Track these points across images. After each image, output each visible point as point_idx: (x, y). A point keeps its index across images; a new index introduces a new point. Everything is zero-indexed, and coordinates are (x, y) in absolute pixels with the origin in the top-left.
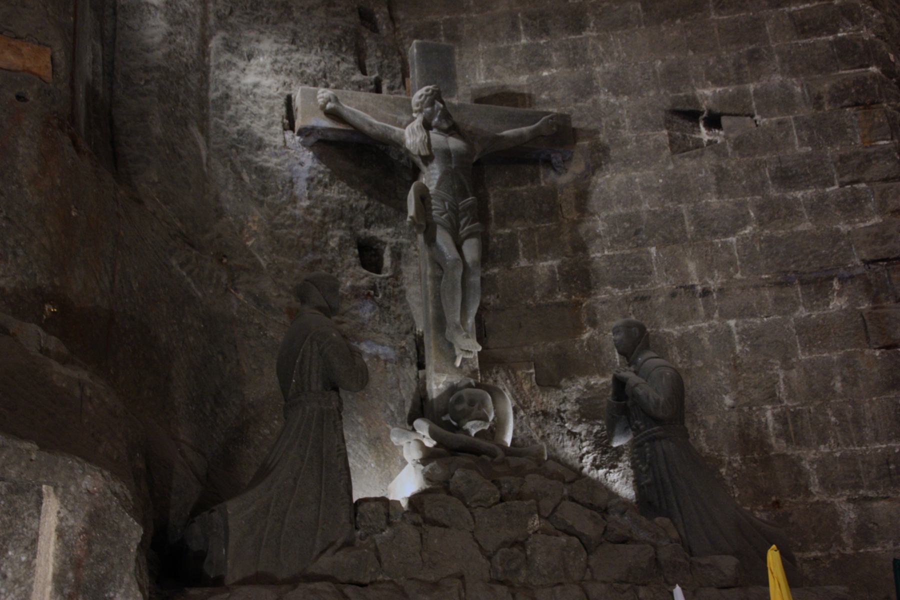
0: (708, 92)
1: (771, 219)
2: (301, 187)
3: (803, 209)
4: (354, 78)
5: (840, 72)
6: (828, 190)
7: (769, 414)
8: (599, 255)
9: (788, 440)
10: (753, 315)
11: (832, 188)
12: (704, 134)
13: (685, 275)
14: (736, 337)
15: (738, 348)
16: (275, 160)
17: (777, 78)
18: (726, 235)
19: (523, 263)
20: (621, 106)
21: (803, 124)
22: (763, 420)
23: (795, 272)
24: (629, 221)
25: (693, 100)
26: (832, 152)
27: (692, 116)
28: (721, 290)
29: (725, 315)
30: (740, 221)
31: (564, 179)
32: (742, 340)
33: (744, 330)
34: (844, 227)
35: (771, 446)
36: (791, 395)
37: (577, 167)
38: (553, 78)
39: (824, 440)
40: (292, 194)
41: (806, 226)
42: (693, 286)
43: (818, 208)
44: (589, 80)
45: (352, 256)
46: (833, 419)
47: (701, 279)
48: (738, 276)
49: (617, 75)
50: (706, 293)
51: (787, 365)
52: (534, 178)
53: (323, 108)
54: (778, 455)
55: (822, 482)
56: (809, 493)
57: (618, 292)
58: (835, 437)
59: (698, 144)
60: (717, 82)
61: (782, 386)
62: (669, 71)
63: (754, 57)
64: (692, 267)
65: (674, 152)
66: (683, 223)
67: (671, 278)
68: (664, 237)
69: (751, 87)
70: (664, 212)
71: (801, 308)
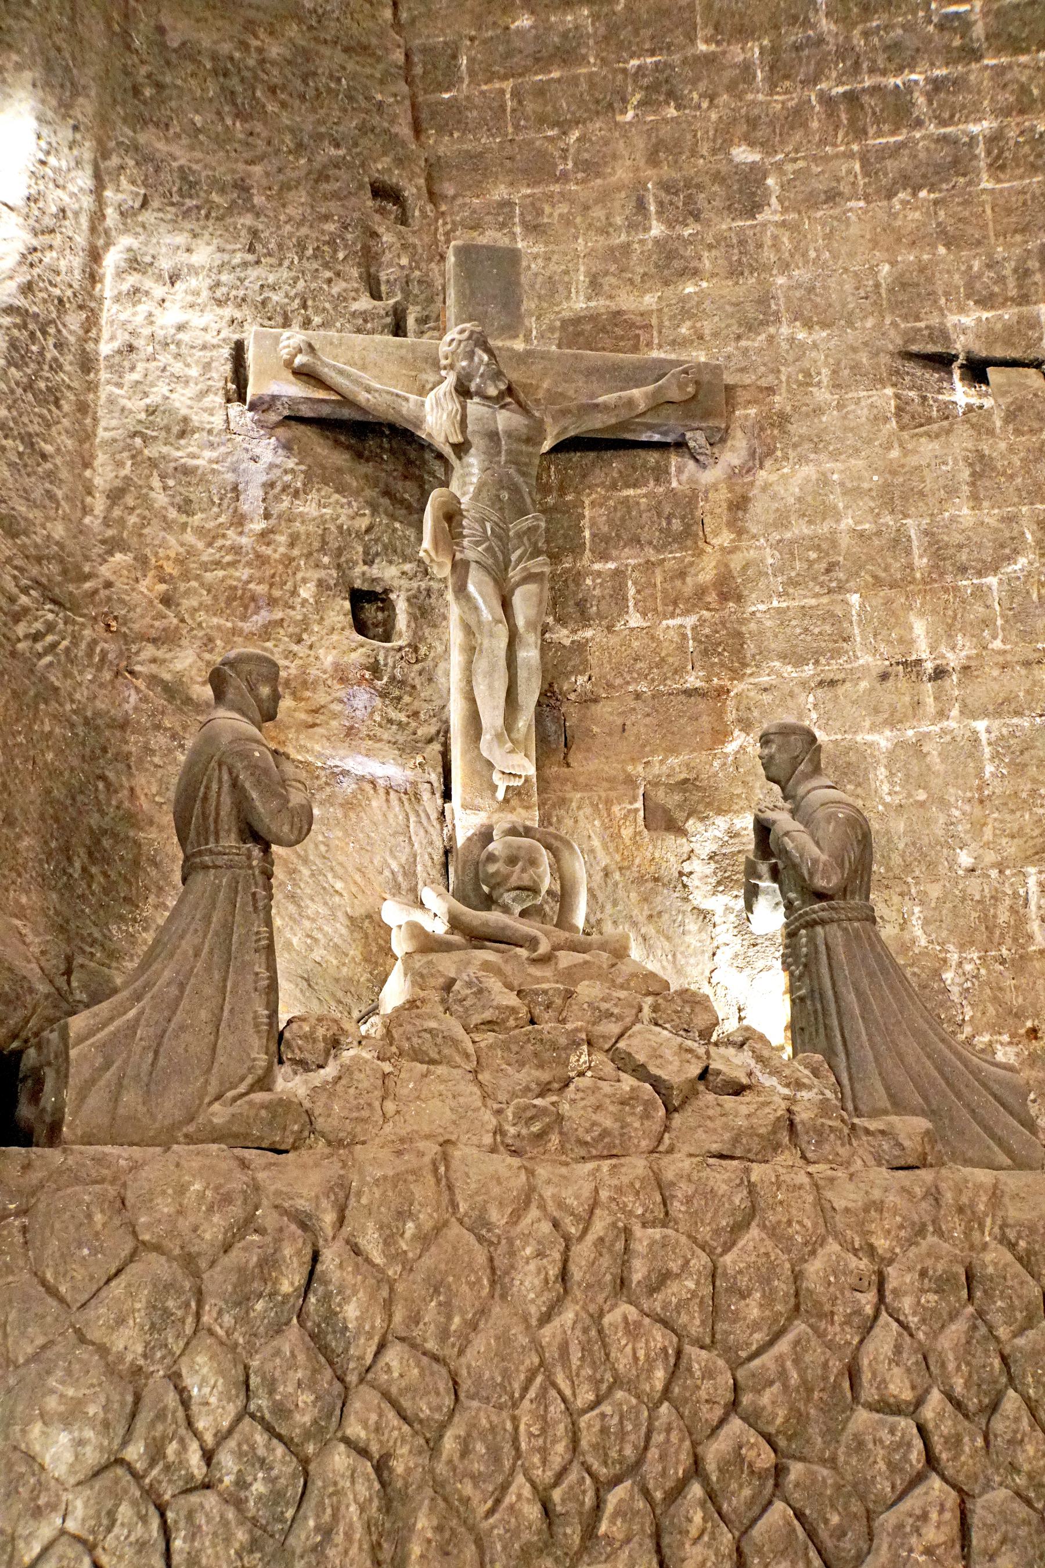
2: (252, 501)
4: (355, 306)
8: (762, 607)
13: (908, 642)
16: (208, 454)
19: (635, 620)
20: (815, 345)
24: (818, 548)
25: (943, 335)
27: (942, 362)
31: (709, 476)
37: (734, 454)
38: (702, 295)
40: (235, 511)
42: (919, 662)
44: (764, 300)
47: (933, 649)
49: (811, 290)
50: (940, 673)
52: (660, 474)
53: (289, 364)
59: (947, 412)
62: (902, 283)
64: (919, 628)
66: (908, 552)
67: (883, 648)
68: (875, 577)
70: (879, 533)
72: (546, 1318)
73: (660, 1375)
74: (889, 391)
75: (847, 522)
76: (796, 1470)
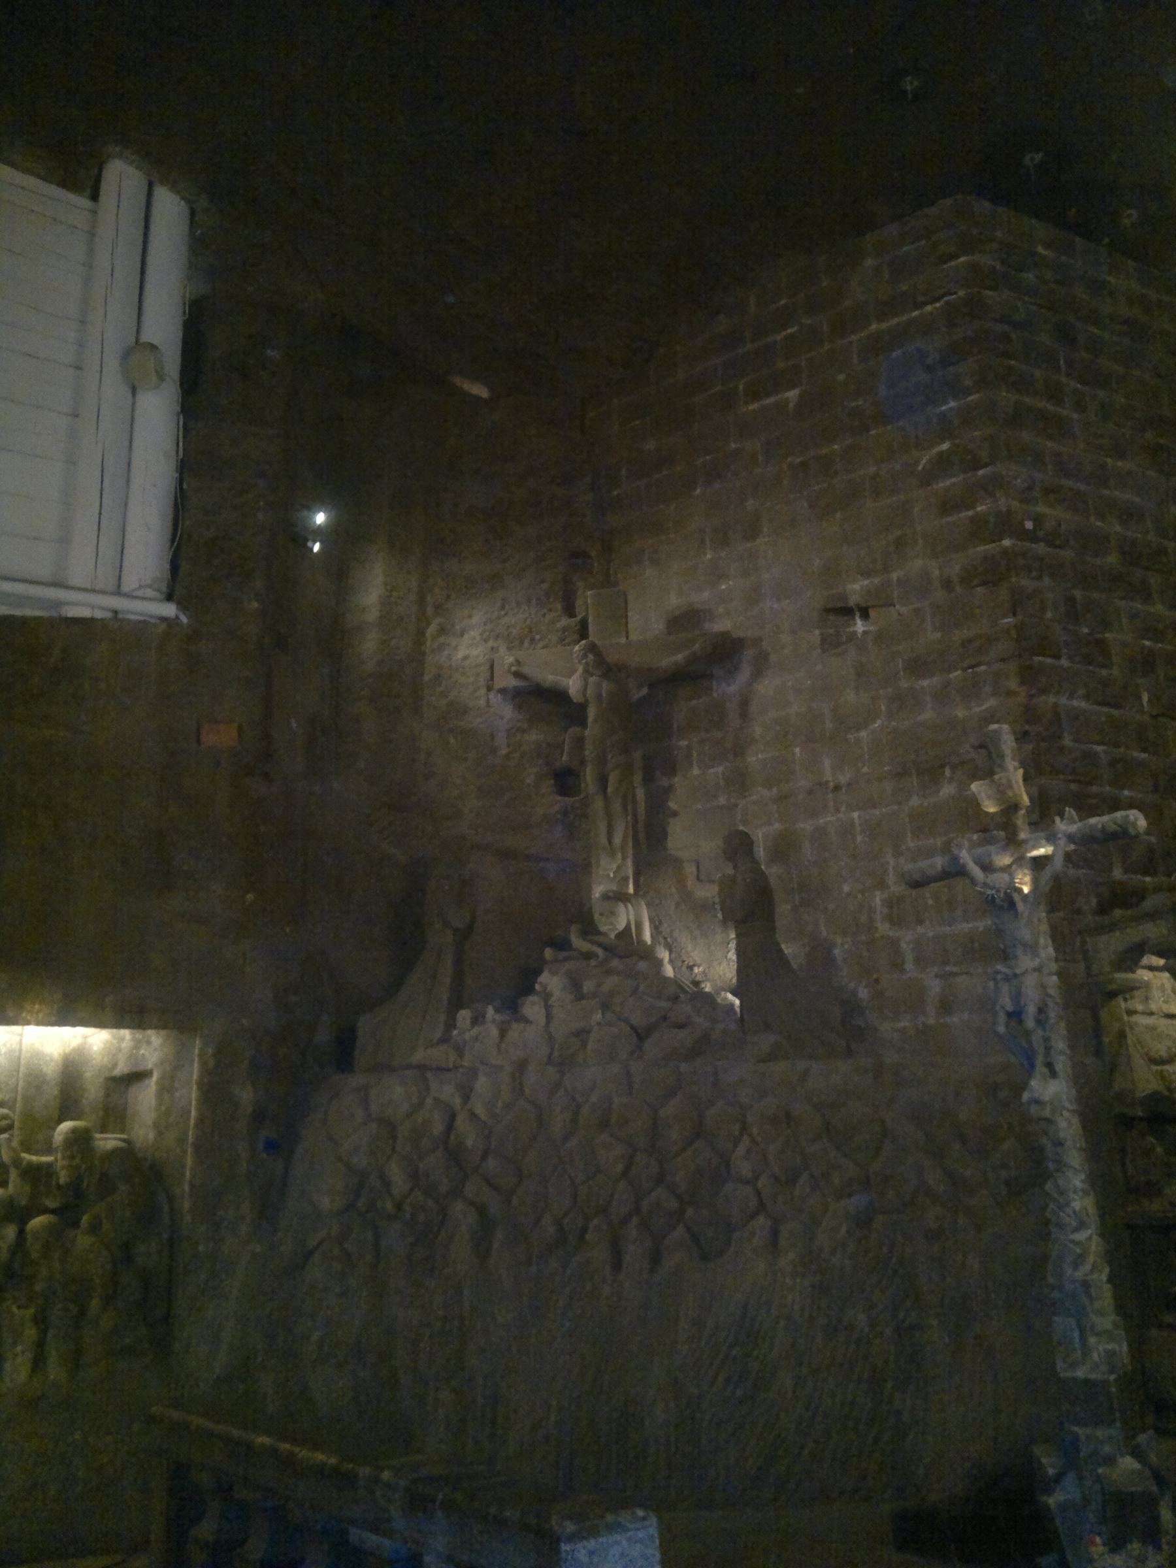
0: (856, 587)
2: (501, 740)
3: (928, 699)
5: (978, 549)
6: (951, 676)
7: (878, 899)
8: (754, 759)
9: (893, 923)
10: (875, 807)
11: (956, 674)
12: (860, 626)
14: (858, 828)
15: (859, 838)
16: (479, 720)
18: (858, 730)
19: (696, 771)
22: (873, 905)
26: (959, 635)
27: (847, 612)
28: (849, 784)
31: (733, 689)
34: (961, 713)
35: (877, 928)
37: (744, 675)
39: (920, 922)
41: (927, 715)
42: (827, 783)
45: (548, 785)
48: (865, 770)
50: (837, 788)
51: (897, 853)
53: (509, 671)
54: (882, 937)
55: (918, 960)
56: (903, 971)
57: (765, 792)
59: (852, 636)
60: (866, 574)
63: (899, 543)
64: (827, 764)
65: (824, 651)
69: (894, 576)
71: (915, 797)
72: (566, 1138)
76: (690, 1211)
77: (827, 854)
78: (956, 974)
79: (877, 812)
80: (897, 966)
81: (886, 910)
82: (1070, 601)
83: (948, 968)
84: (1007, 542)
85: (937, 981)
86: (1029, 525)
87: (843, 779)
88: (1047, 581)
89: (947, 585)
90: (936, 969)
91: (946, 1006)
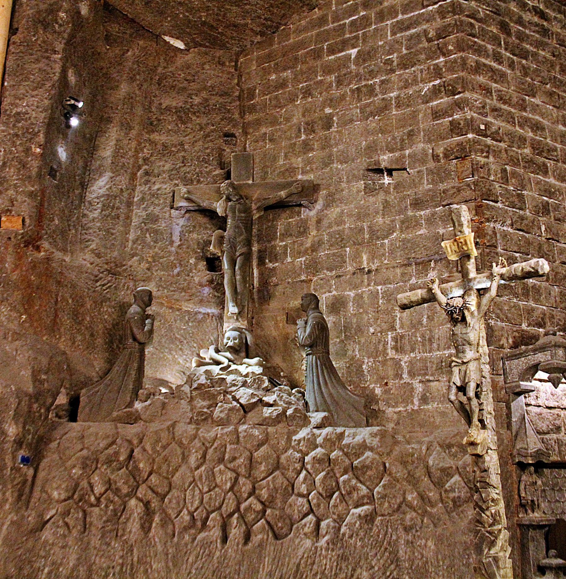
0: (385, 157)
1: (407, 228)
4: (214, 173)
9: (397, 350)
12: (387, 180)
13: (361, 262)
14: (381, 295)
15: (381, 301)
17: (421, 145)
19: (289, 259)
20: (343, 170)
21: (430, 172)
23: (414, 258)
24: (339, 234)
25: (378, 163)
26: (442, 186)
27: (379, 171)
28: (377, 270)
29: (376, 284)
30: (391, 231)
31: (313, 213)
32: (383, 297)
33: (385, 292)
36: (402, 327)
37: (319, 206)
38: (313, 157)
39: (413, 350)
43: (430, 221)
44: (330, 156)
45: (202, 265)
46: (419, 339)
47: (368, 264)
48: (386, 262)
49: (343, 152)
50: (369, 272)
52: (299, 213)
54: (391, 359)
55: (409, 372)
56: (401, 378)
57: (329, 273)
58: (419, 349)
59: (382, 186)
60: (391, 151)
61: (398, 322)
62: (369, 147)
63: (410, 134)
64: (365, 257)
65: (366, 193)
67: (354, 265)
68: (354, 242)
69: (407, 152)
70: (356, 228)
71: (414, 278)
72: (198, 468)
73: (229, 485)
74: (362, 182)
75: (347, 225)
76: (269, 511)
77: (361, 310)
78: (433, 381)
79: (392, 286)
80: (398, 376)
81: (393, 343)
82: (504, 171)
83: (427, 377)
84: (470, 136)
85: (421, 385)
86: (482, 127)
87: (374, 267)
88: (491, 159)
89: (436, 157)
90: (420, 378)
91: (424, 400)
